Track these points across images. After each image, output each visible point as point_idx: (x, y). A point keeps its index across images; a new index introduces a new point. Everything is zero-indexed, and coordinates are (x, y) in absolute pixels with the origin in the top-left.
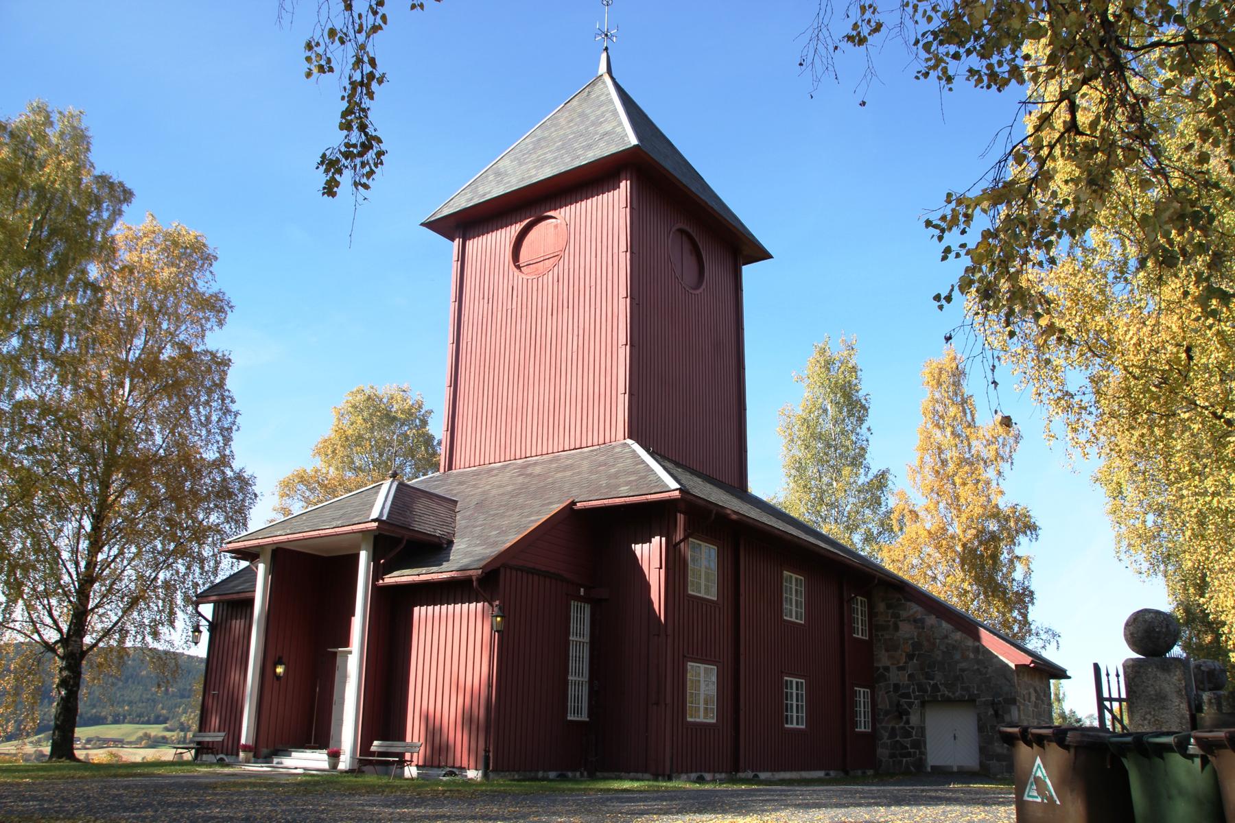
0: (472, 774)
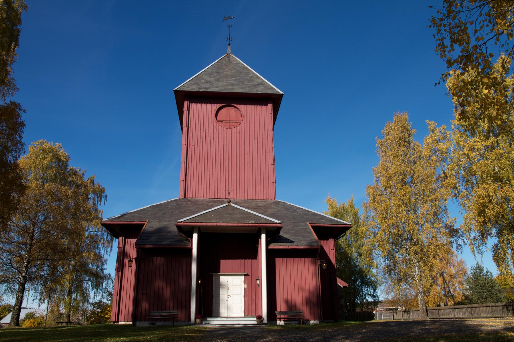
0: (312, 322)
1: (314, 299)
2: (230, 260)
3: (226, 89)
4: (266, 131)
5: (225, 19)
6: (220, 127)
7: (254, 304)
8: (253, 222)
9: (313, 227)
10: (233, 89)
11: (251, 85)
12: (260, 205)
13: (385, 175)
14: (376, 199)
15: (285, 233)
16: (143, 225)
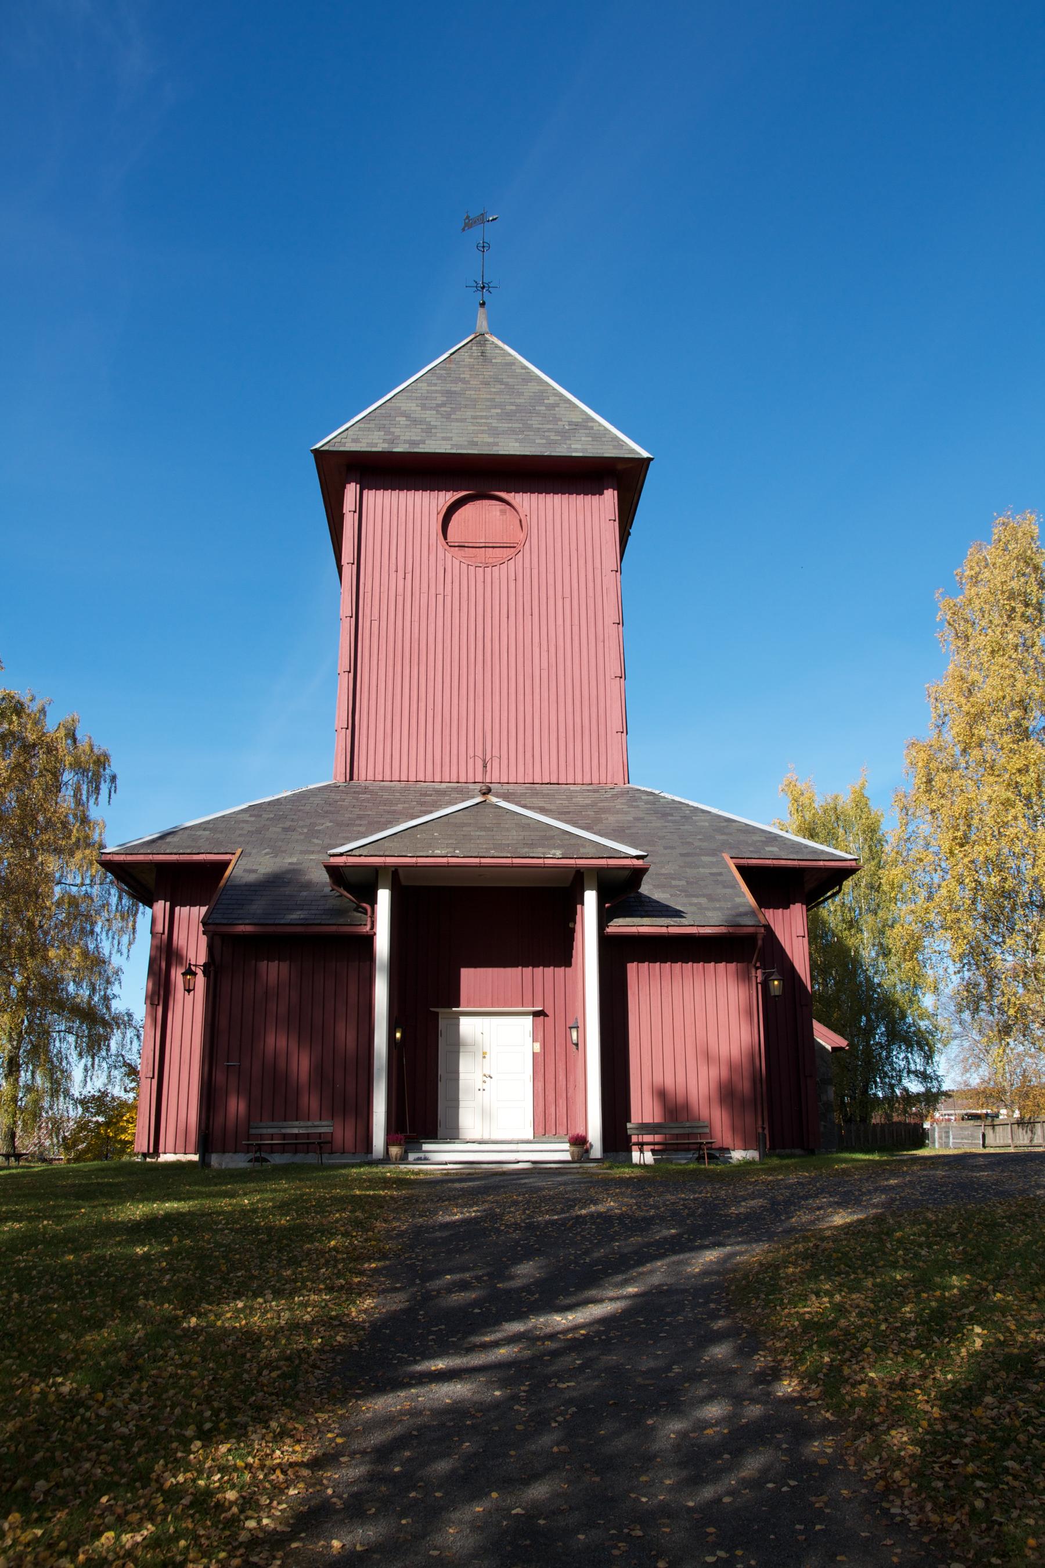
0: (737, 1155)
1: (745, 1086)
2: (490, 970)
3: (476, 444)
4: (598, 572)
5: (469, 223)
6: (456, 563)
7: (562, 1103)
8: (558, 853)
9: (740, 868)
10: (496, 444)
11: (549, 430)
12: (579, 800)
13: (965, 708)
14: (937, 784)
15: (656, 887)
16: (225, 864)
